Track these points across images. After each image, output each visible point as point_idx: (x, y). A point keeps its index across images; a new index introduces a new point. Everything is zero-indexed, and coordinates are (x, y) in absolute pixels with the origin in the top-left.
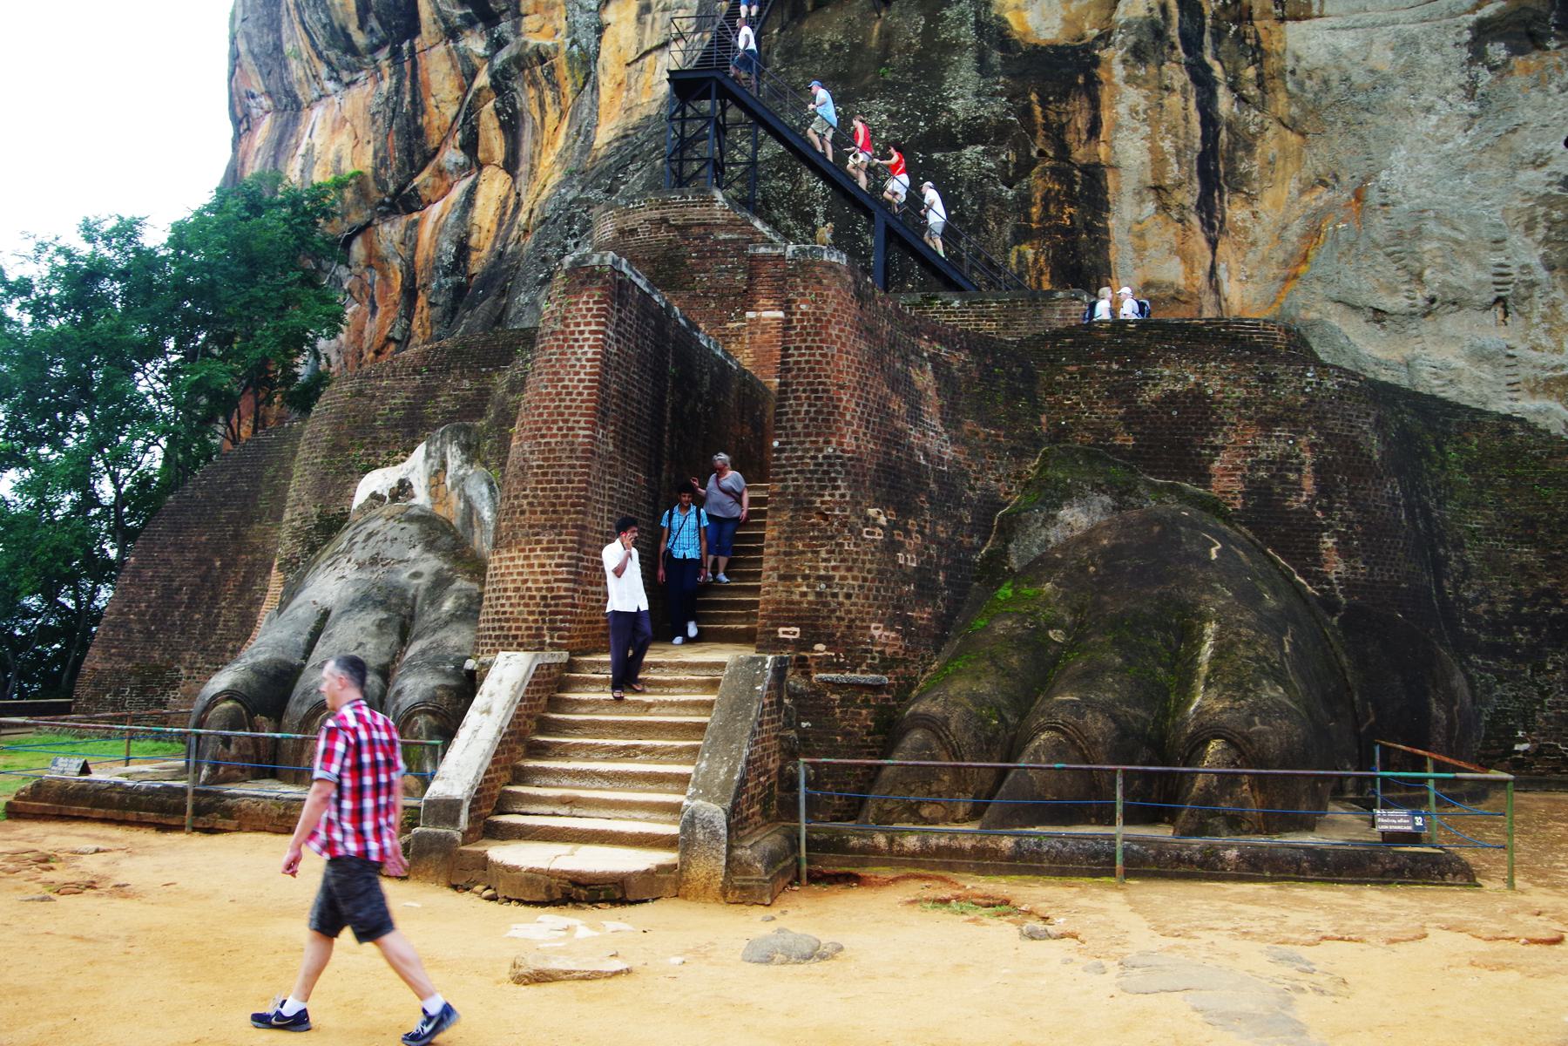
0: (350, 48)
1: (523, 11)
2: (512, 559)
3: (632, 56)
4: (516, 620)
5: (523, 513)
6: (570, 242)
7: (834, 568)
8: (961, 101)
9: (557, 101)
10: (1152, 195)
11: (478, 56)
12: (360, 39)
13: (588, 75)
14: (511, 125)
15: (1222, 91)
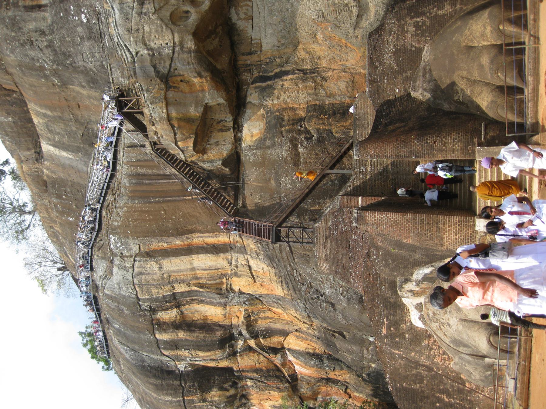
0: (234, 397)
1: (230, 324)
2: (447, 237)
3: (252, 281)
4: (466, 234)
5: (432, 234)
6: (321, 298)
7: (451, 138)
8: (283, 153)
9: (264, 312)
10: (317, 90)
11: (244, 343)
12: (232, 392)
13: (256, 298)
14: (269, 333)
15: (283, 69)
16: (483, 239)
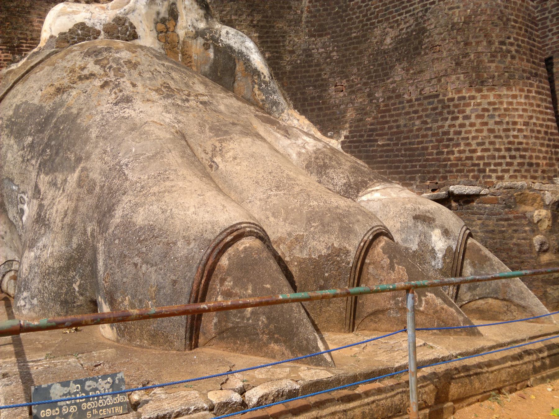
2: (515, 97)
4: (534, 150)
16: (534, 200)
